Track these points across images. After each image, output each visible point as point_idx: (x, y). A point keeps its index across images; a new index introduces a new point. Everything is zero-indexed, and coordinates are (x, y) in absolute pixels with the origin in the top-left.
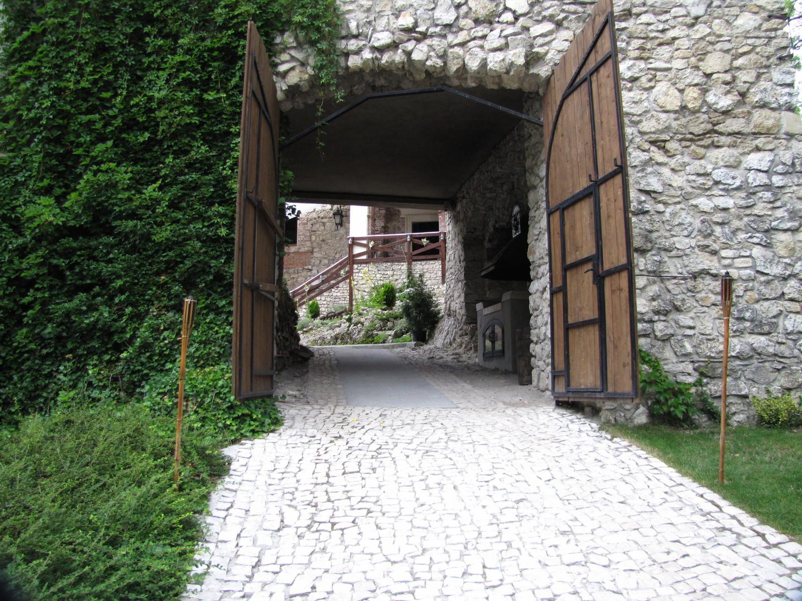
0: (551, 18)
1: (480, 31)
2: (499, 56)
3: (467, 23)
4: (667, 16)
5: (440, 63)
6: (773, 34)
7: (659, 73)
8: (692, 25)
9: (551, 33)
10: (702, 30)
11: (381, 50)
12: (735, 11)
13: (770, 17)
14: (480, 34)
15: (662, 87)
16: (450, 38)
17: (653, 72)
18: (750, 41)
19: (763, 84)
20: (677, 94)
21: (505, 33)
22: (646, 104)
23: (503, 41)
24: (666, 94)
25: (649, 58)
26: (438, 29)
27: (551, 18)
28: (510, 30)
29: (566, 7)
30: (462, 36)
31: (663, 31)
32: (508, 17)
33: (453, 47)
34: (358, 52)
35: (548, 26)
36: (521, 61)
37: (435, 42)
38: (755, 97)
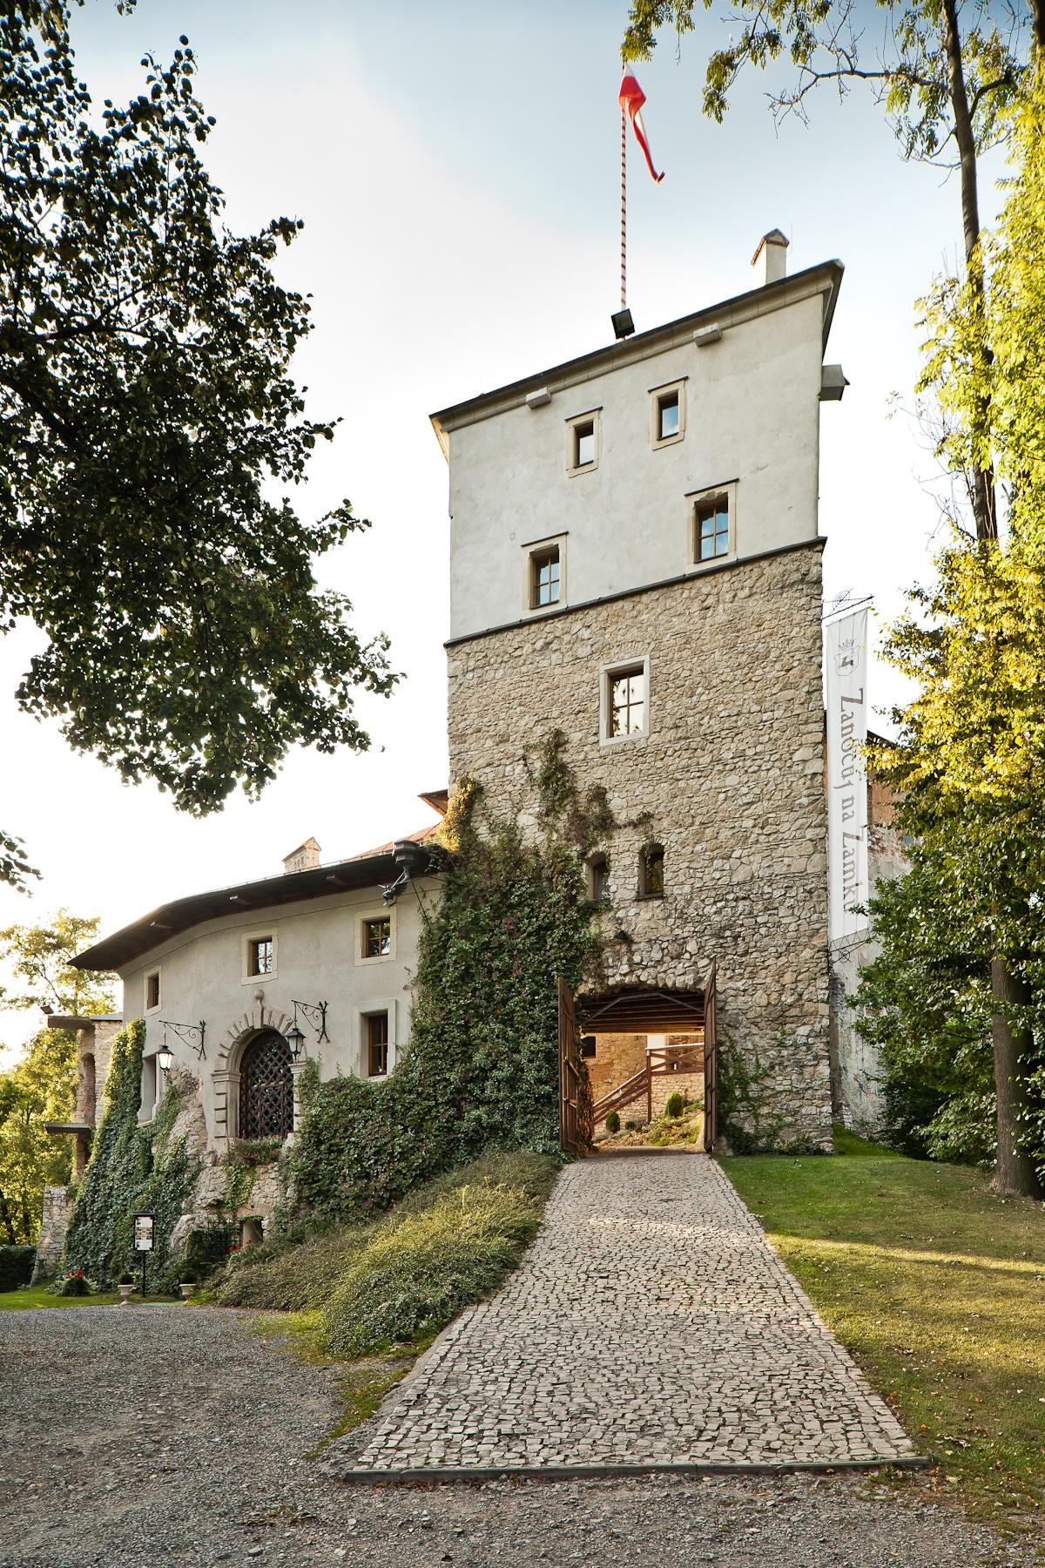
0: (708, 956)
1: (672, 964)
3: (667, 959)
10: (783, 959)
19: (811, 988)
27: (708, 956)
35: (706, 961)
36: (691, 983)
38: (805, 997)
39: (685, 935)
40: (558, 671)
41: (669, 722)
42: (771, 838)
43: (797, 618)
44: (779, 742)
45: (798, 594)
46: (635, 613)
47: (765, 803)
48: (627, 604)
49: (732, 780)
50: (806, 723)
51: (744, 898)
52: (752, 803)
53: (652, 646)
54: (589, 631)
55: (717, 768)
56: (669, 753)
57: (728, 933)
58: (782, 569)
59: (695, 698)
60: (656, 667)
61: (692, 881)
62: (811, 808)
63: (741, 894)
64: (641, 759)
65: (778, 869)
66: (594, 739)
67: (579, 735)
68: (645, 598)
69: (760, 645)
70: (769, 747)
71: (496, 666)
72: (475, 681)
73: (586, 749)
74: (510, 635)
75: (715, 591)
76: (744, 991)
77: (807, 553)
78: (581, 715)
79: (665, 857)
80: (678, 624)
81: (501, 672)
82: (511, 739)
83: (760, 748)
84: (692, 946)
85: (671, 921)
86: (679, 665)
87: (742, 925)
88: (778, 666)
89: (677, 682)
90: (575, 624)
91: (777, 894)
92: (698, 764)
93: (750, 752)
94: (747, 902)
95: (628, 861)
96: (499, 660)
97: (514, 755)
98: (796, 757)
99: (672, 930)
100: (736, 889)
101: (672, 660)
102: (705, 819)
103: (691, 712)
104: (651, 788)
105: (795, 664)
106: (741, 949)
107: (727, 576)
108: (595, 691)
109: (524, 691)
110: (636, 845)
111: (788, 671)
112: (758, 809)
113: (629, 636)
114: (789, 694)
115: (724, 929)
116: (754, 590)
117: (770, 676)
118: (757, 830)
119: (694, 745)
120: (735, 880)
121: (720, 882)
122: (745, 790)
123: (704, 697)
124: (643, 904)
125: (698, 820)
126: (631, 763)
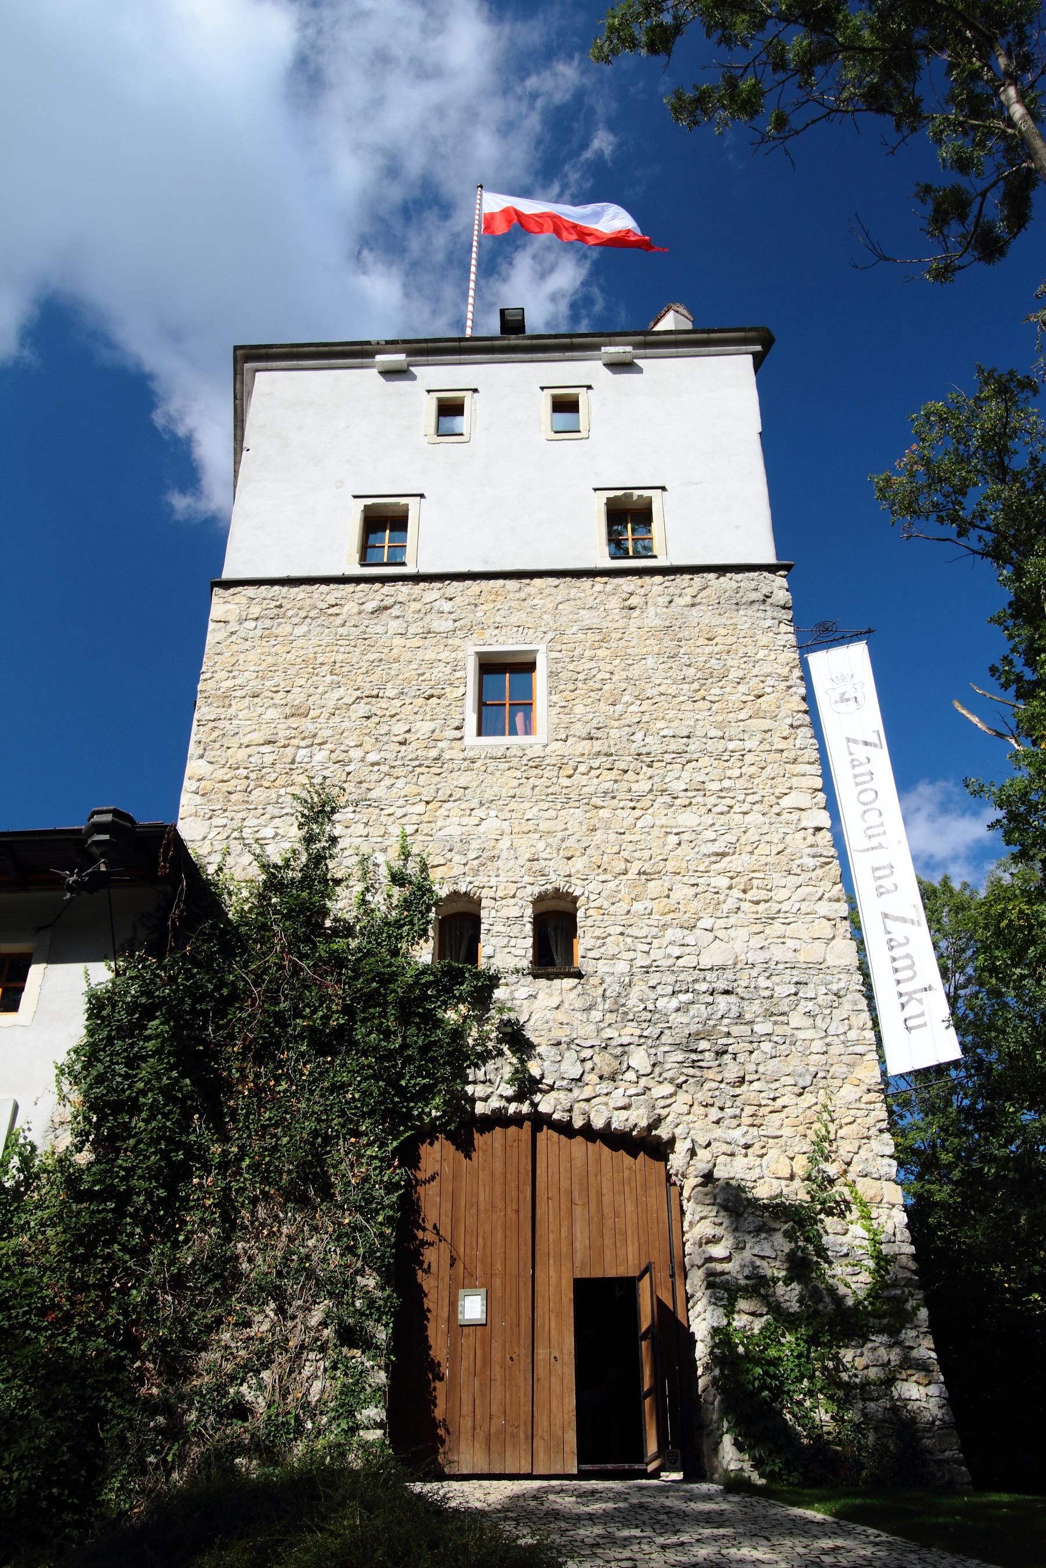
0: (672, 1081)
1: (605, 1086)
2: (624, 1114)
3: (592, 1078)
4: (776, 1085)
5: (566, 1117)
6: (872, 1107)
7: (770, 1140)
8: (801, 1094)
9: (672, 1095)
10: (808, 1099)
11: (509, 1100)
12: (838, 1082)
13: (869, 1091)
14: (605, 1091)
15: (773, 1153)
16: (576, 1092)
17: (765, 1139)
18: (852, 1112)
20: (788, 1160)
21: (629, 1092)
22: (758, 1170)
23: (626, 1101)
24: (777, 1161)
25: (762, 1125)
26: (565, 1082)
27: (672, 1081)
28: (632, 1091)
29: (685, 1070)
30: (587, 1092)
31: (774, 1099)
32: (631, 1076)
33: (579, 1101)
34: (485, 1099)
35: (668, 1089)
37: (562, 1095)
39: (625, 1040)
40: (398, 641)
41: (579, 729)
42: (762, 907)
43: (764, 640)
44: (756, 781)
45: (761, 614)
46: (522, 595)
47: (745, 857)
48: (512, 584)
49: (687, 819)
50: (795, 761)
51: (727, 992)
52: (723, 855)
53: (550, 635)
54: (450, 603)
55: (661, 800)
56: (582, 768)
57: (703, 1045)
58: (734, 585)
59: (619, 708)
60: (557, 661)
61: (631, 955)
62: (819, 872)
63: (721, 985)
64: (536, 771)
65: (779, 953)
66: (458, 734)
67: (428, 726)
68: (537, 582)
69: (713, 661)
70: (741, 783)
71: (296, 620)
72: (258, 632)
73: (440, 744)
74: (324, 588)
75: (643, 591)
76: (747, 1147)
77: (766, 574)
78: (434, 700)
79: (580, 914)
80: (588, 618)
81: (303, 629)
82: (312, 714)
83: (726, 783)
84: (639, 1059)
85: (595, 1015)
86: (592, 664)
87: (728, 1034)
88: (742, 688)
89: (591, 683)
90: (432, 592)
91: (782, 991)
92: (630, 790)
93: (715, 786)
94: (732, 999)
95: (515, 912)
96: (303, 614)
97: (315, 736)
98: (786, 802)
99: (599, 1031)
100: (709, 976)
101: (582, 657)
102: (647, 867)
103: (616, 724)
104: (552, 813)
105: (769, 690)
106: (732, 1072)
107: (658, 579)
108: (458, 674)
109: (340, 657)
110: (529, 889)
111: (759, 697)
112: (734, 863)
113: (513, 619)
114: (766, 724)
115: (698, 1036)
116: (698, 600)
117: (733, 698)
118: (736, 893)
119: (623, 766)
120: (706, 962)
121: (680, 962)
122: (710, 834)
123: (632, 708)
124: (543, 982)
125: (634, 869)
126: (518, 774)
